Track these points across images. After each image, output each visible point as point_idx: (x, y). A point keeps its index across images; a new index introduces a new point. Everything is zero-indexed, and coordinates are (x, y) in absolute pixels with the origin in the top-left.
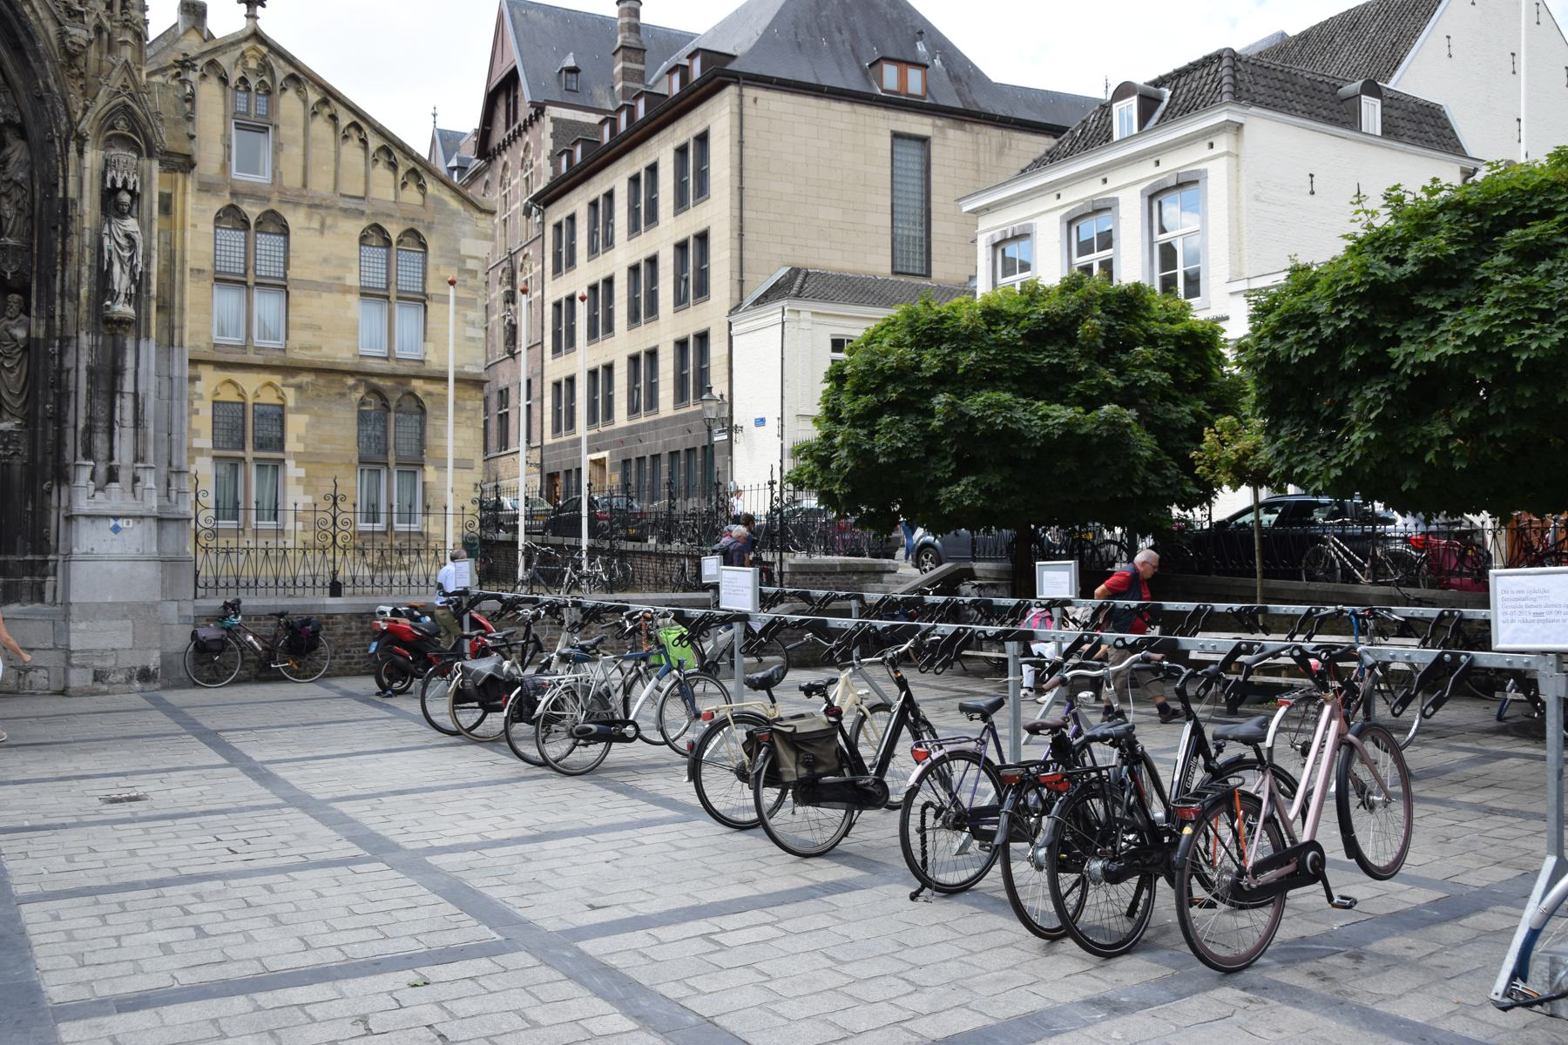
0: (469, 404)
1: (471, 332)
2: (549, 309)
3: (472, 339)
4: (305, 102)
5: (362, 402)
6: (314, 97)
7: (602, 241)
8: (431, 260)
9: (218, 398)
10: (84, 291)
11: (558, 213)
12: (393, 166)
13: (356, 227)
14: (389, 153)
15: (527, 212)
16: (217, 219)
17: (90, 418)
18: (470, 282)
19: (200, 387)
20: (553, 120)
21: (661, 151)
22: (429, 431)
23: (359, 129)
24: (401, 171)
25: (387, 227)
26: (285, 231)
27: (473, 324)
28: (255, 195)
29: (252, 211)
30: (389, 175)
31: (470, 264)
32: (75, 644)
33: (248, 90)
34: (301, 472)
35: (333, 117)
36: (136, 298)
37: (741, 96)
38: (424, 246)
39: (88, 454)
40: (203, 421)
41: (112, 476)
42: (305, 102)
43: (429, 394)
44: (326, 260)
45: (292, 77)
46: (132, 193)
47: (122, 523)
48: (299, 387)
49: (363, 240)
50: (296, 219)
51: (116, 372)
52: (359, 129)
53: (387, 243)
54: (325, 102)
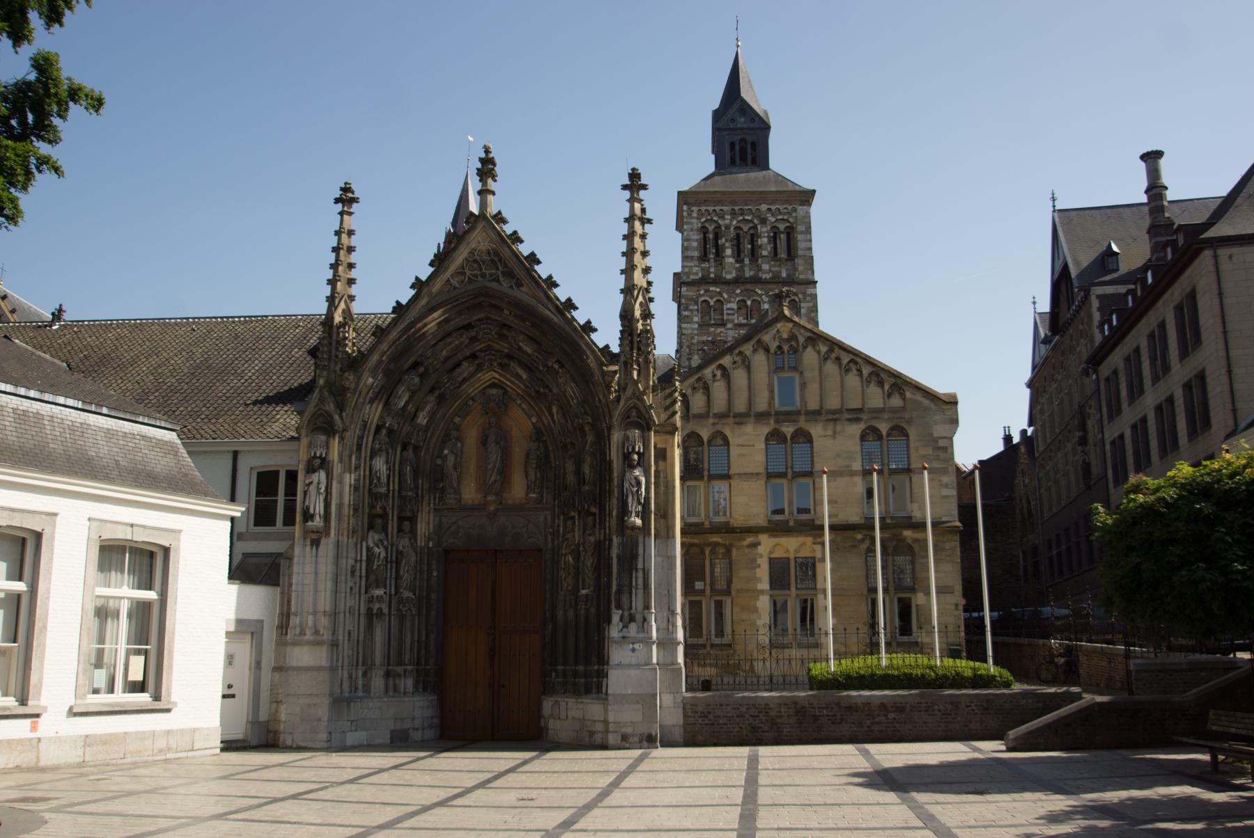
0: (947, 545)
1: (945, 492)
2: (1108, 447)
3: (947, 497)
4: (819, 352)
6: (824, 349)
7: (1136, 391)
8: (912, 444)
9: (773, 556)
10: (615, 513)
11: (1105, 369)
12: (881, 383)
13: (856, 430)
14: (878, 375)
15: (1086, 373)
16: (767, 439)
17: (619, 585)
19: (760, 549)
20: (1099, 297)
21: (1165, 310)
22: (918, 567)
23: (856, 363)
24: (887, 387)
26: (809, 440)
27: (946, 486)
28: (789, 416)
29: (788, 430)
30: (879, 390)
31: (942, 443)
32: (611, 719)
33: (783, 352)
35: (838, 359)
36: (645, 515)
37: (1216, 257)
38: (907, 435)
39: (619, 607)
40: (763, 572)
41: (632, 619)
42: (819, 352)
44: (838, 456)
45: (809, 338)
46: (638, 453)
47: (637, 646)
49: (863, 438)
50: (816, 430)
51: (634, 557)
53: (880, 437)
54: (831, 350)
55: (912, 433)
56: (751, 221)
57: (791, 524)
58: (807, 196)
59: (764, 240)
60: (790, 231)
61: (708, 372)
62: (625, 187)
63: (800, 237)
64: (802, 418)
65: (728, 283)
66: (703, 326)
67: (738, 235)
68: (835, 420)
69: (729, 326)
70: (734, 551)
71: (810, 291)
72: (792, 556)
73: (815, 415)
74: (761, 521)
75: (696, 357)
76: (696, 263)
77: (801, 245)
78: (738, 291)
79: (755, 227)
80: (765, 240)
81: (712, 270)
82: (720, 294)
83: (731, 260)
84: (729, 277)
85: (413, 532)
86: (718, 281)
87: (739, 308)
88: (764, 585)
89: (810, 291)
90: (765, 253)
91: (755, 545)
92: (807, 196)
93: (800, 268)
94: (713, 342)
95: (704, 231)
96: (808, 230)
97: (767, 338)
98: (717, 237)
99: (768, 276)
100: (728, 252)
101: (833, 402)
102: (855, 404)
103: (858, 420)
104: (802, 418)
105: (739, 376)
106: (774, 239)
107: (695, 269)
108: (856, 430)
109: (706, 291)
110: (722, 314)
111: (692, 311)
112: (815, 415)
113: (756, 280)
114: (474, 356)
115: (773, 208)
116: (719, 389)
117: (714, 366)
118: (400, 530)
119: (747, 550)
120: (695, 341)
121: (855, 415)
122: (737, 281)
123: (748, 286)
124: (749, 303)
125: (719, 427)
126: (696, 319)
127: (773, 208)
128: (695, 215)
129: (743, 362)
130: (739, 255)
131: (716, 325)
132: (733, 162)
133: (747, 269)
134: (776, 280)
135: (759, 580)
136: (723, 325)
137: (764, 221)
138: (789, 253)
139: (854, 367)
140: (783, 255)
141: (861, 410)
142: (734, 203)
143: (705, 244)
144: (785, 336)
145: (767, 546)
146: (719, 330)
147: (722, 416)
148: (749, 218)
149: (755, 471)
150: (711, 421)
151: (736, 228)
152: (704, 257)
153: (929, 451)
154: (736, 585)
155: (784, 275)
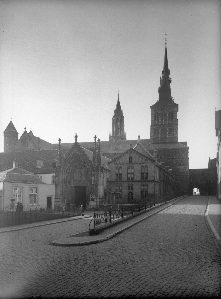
62: (94, 138)
65: (159, 125)
69: (160, 134)
79: (165, 113)
81: (157, 123)
84: (160, 124)
85: (70, 184)
100: (160, 119)
102: (140, 162)
114: (76, 161)
118: (68, 184)
122: (162, 125)
126: (153, 133)
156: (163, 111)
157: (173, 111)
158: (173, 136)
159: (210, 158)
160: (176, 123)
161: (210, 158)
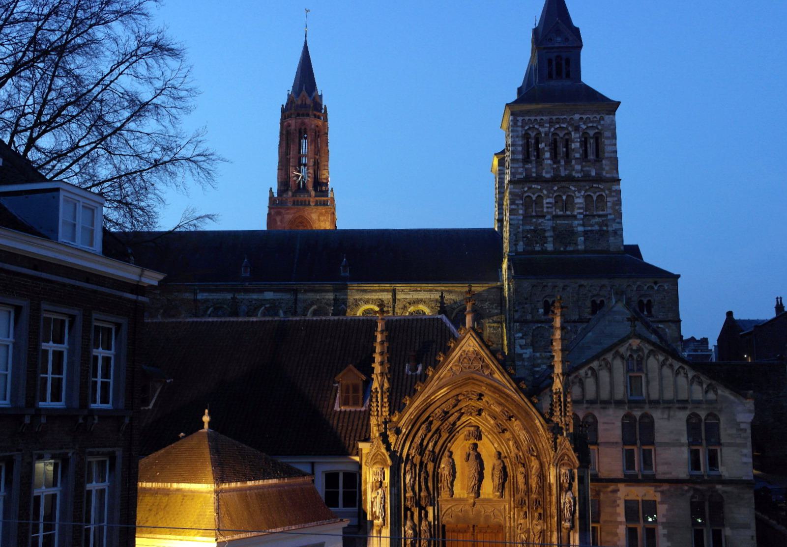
1: (745, 460)
3: (745, 463)
4: (658, 360)
5: (693, 497)
9: (627, 498)
12: (701, 383)
13: (683, 415)
14: (699, 378)
18: (743, 435)
19: (619, 494)
23: (683, 368)
25: (699, 413)
27: (745, 455)
31: (743, 426)
33: (633, 359)
34: (665, 531)
35: (671, 366)
38: (719, 420)
40: (621, 510)
42: (658, 360)
43: (725, 492)
48: (662, 492)
52: (683, 368)
55: (723, 419)
56: (567, 128)
57: (640, 477)
58: (612, 106)
59: (575, 145)
60: (598, 137)
61: (582, 372)
63: (607, 142)
64: (647, 406)
65: (546, 181)
66: (527, 217)
67: (555, 141)
68: (669, 408)
69: (548, 217)
70: (602, 494)
71: (615, 188)
72: (640, 499)
73: (655, 403)
74: (619, 474)
75: (521, 243)
76: (521, 164)
77: (608, 149)
78: (556, 188)
79: (569, 133)
80: (578, 144)
82: (541, 190)
83: (549, 162)
84: (548, 176)
86: (539, 179)
87: (556, 202)
88: (622, 518)
89: (615, 188)
90: (577, 155)
91: (616, 491)
92: (612, 106)
93: (607, 168)
94: (535, 231)
95: (526, 136)
96: (614, 136)
97: (622, 349)
98: (537, 142)
99: (580, 175)
100: (547, 155)
101: (669, 395)
102: (683, 396)
103: (685, 408)
104: (647, 406)
105: (604, 375)
106: (584, 143)
107: (520, 170)
108: (683, 415)
109: (529, 188)
110: (542, 207)
111: (517, 205)
112: (655, 403)
113: (570, 179)
115: (584, 117)
116: (590, 383)
117: (586, 368)
119: (610, 494)
120: (520, 230)
121: (683, 404)
122: (555, 179)
123: (564, 184)
124: (564, 198)
125: (590, 410)
127: (584, 117)
128: (520, 124)
129: (606, 365)
130: (556, 157)
131: (538, 217)
132: (550, 76)
133: (562, 169)
134: (587, 178)
135: (619, 514)
136: (544, 217)
137: (577, 129)
138: (597, 155)
139: (682, 371)
140: (591, 157)
141: (686, 401)
142: (551, 113)
143: (528, 149)
144: (635, 348)
145: (626, 492)
146: (540, 220)
147: (592, 402)
148: (564, 126)
149: (615, 441)
150: (585, 405)
151: (554, 134)
152: (526, 160)
153: (734, 431)
154: (603, 518)
155: (593, 174)
156: (558, 126)
157: (599, 127)
158: (605, 228)
159: (730, 314)
160: (615, 175)
161: (730, 314)
